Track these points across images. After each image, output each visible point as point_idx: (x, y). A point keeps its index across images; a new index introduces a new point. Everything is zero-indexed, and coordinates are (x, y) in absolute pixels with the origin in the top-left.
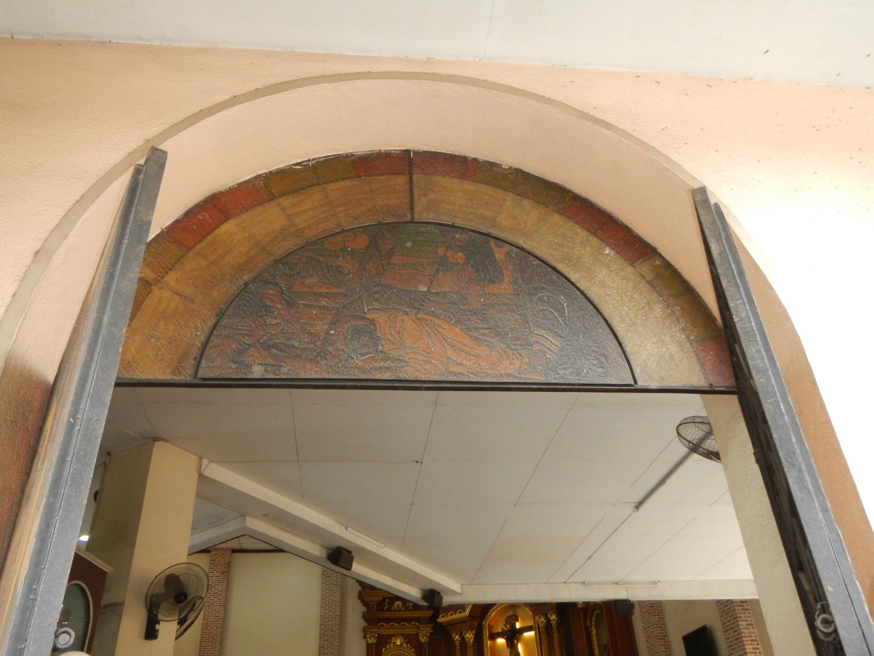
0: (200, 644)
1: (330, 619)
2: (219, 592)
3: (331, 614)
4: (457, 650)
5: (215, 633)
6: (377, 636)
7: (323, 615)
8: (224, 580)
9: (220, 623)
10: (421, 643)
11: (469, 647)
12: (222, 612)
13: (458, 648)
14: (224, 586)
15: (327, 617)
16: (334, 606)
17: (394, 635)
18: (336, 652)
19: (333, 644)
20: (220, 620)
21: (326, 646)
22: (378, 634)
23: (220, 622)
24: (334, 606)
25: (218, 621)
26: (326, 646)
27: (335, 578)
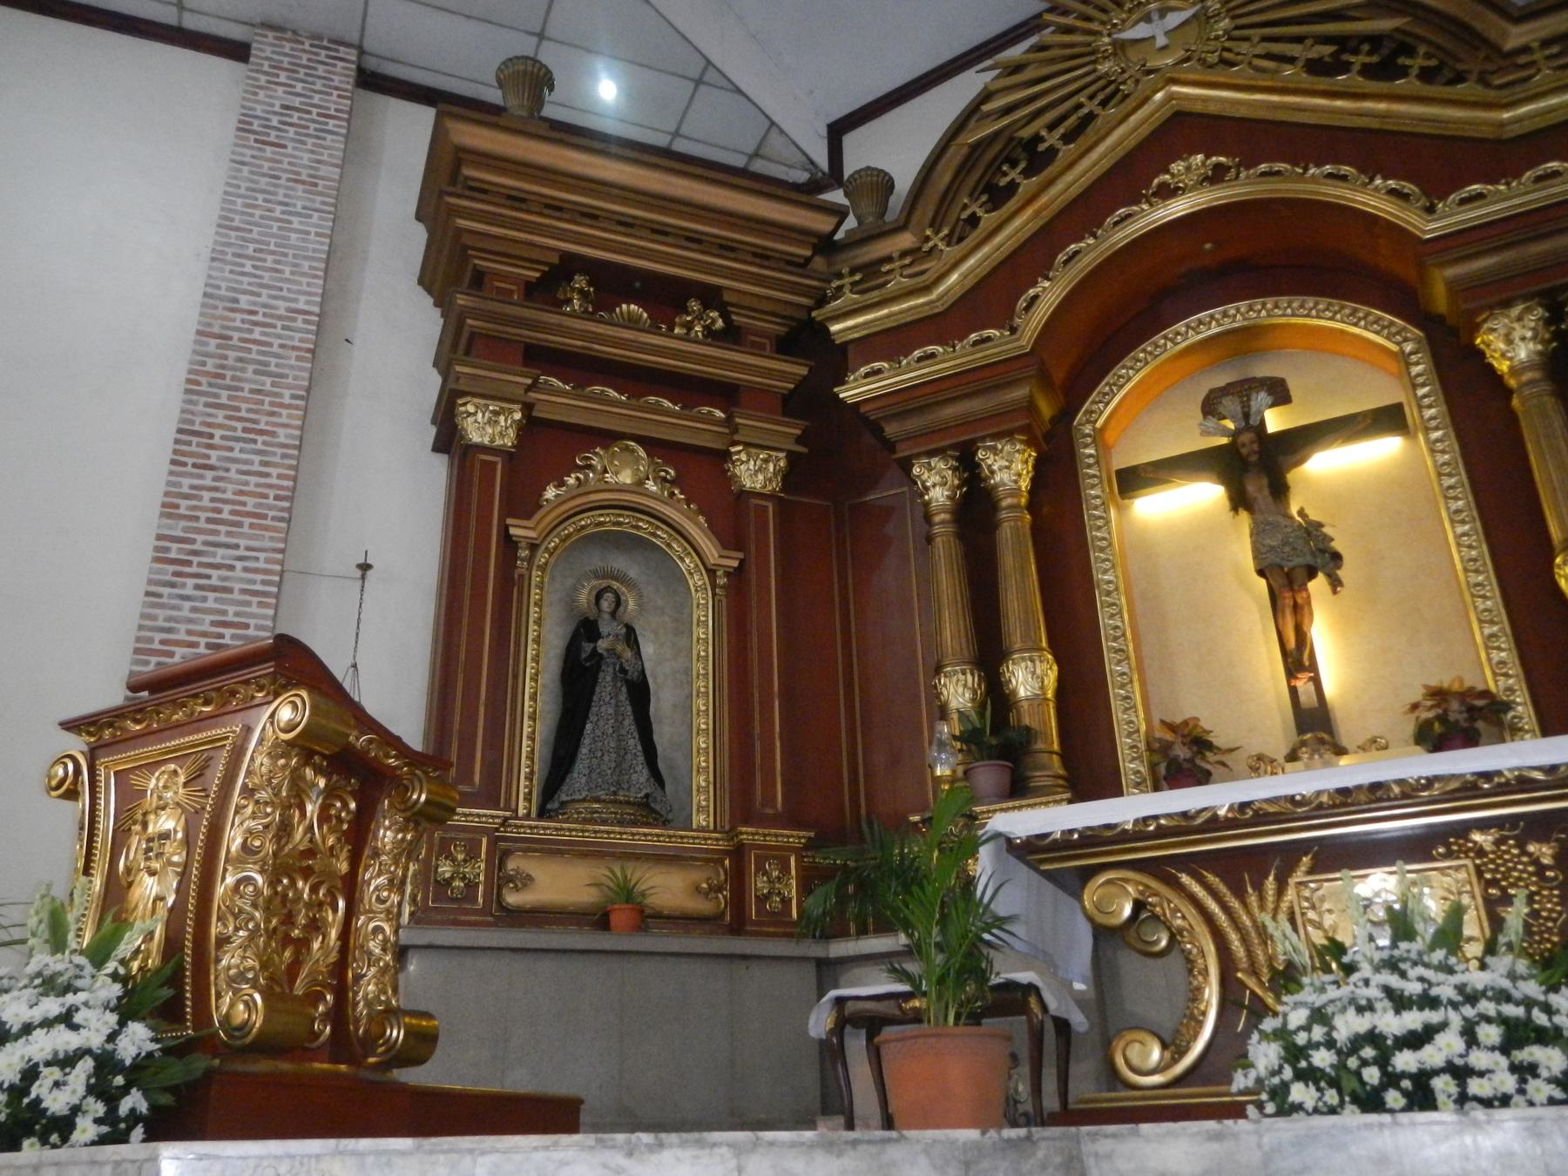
1: (259, 318)
3: (264, 299)
4: (937, 530)
6: (518, 416)
10: (744, 495)
11: (1011, 507)
13: (937, 519)
15: (243, 305)
16: (287, 270)
17: (608, 438)
18: (274, 471)
19: (262, 432)
21: (218, 433)
22: (528, 408)
24: (287, 270)
26: (218, 433)
27: (306, 156)
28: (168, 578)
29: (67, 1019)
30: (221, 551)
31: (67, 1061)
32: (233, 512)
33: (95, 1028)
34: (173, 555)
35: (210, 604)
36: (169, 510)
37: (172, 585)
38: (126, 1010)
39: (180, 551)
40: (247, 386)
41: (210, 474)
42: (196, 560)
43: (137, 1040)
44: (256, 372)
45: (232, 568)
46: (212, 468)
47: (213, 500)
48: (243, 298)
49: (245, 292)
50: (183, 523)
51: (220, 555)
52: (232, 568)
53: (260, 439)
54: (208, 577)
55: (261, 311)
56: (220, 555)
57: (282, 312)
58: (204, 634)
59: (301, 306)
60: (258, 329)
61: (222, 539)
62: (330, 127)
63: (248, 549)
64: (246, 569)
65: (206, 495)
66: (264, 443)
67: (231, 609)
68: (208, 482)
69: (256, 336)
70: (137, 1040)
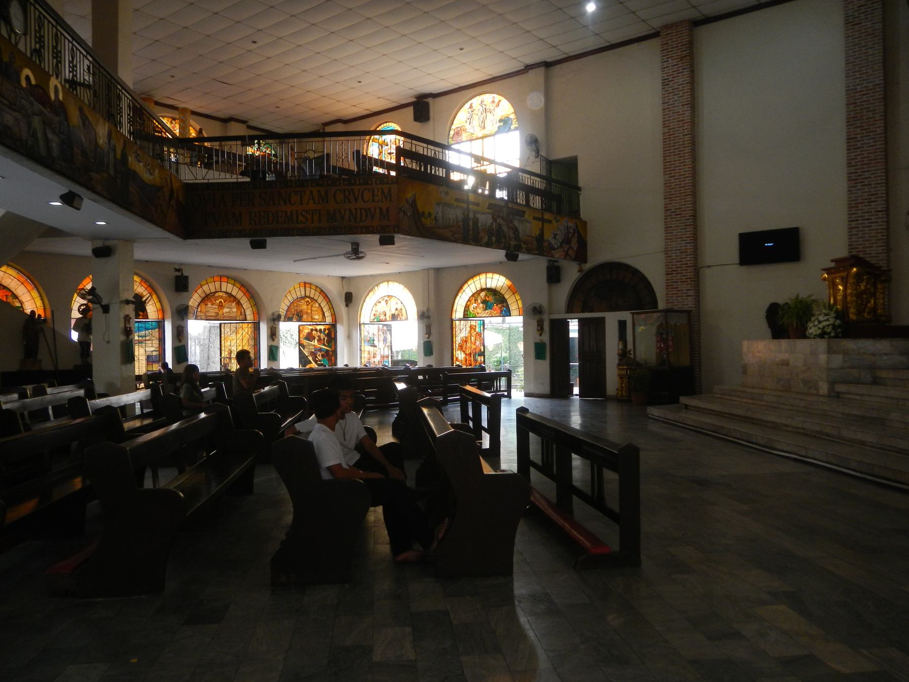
0: (664, 160)
2: (680, 87)
3: (865, 85)
5: (681, 143)
7: (851, 88)
8: (684, 69)
9: (687, 129)
12: (688, 113)
14: (685, 76)
20: (686, 125)
23: (686, 127)
24: (870, 71)
25: (684, 126)
28: (853, 185)
29: (828, 320)
30: (866, 173)
31: (828, 325)
32: (868, 160)
33: (832, 321)
34: (853, 178)
35: (866, 190)
36: (849, 165)
37: (854, 187)
38: (836, 318)
39: (855, 176)
40: (865, 117)
41: (858, 150)
42: (859, 178)
43: (838, 322)
44: (867, 112)
45: (870, 178)
46: (859, 148)
47: (861, 158)
48: (858, 87)
49: (858, 85)
50: (854, 168)
51: (867, 174)
52: (870, 178)
53: (872, 134)
54: (864, 182)
55: (864, 89)
56: (867, 174)
57: (871, 87)
58: (866, 199)
59: (877, 83)
60: (865, 97)
61: (866, 169)
62: (876, 7)
63: (875, 170)
64: (874, 177)
65: (859, 157)
66: (873, 135)
67: (872, 190)
68: (859, 153)
69: (865, 99)
70: (838, 322)
